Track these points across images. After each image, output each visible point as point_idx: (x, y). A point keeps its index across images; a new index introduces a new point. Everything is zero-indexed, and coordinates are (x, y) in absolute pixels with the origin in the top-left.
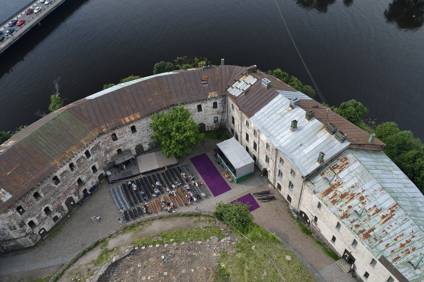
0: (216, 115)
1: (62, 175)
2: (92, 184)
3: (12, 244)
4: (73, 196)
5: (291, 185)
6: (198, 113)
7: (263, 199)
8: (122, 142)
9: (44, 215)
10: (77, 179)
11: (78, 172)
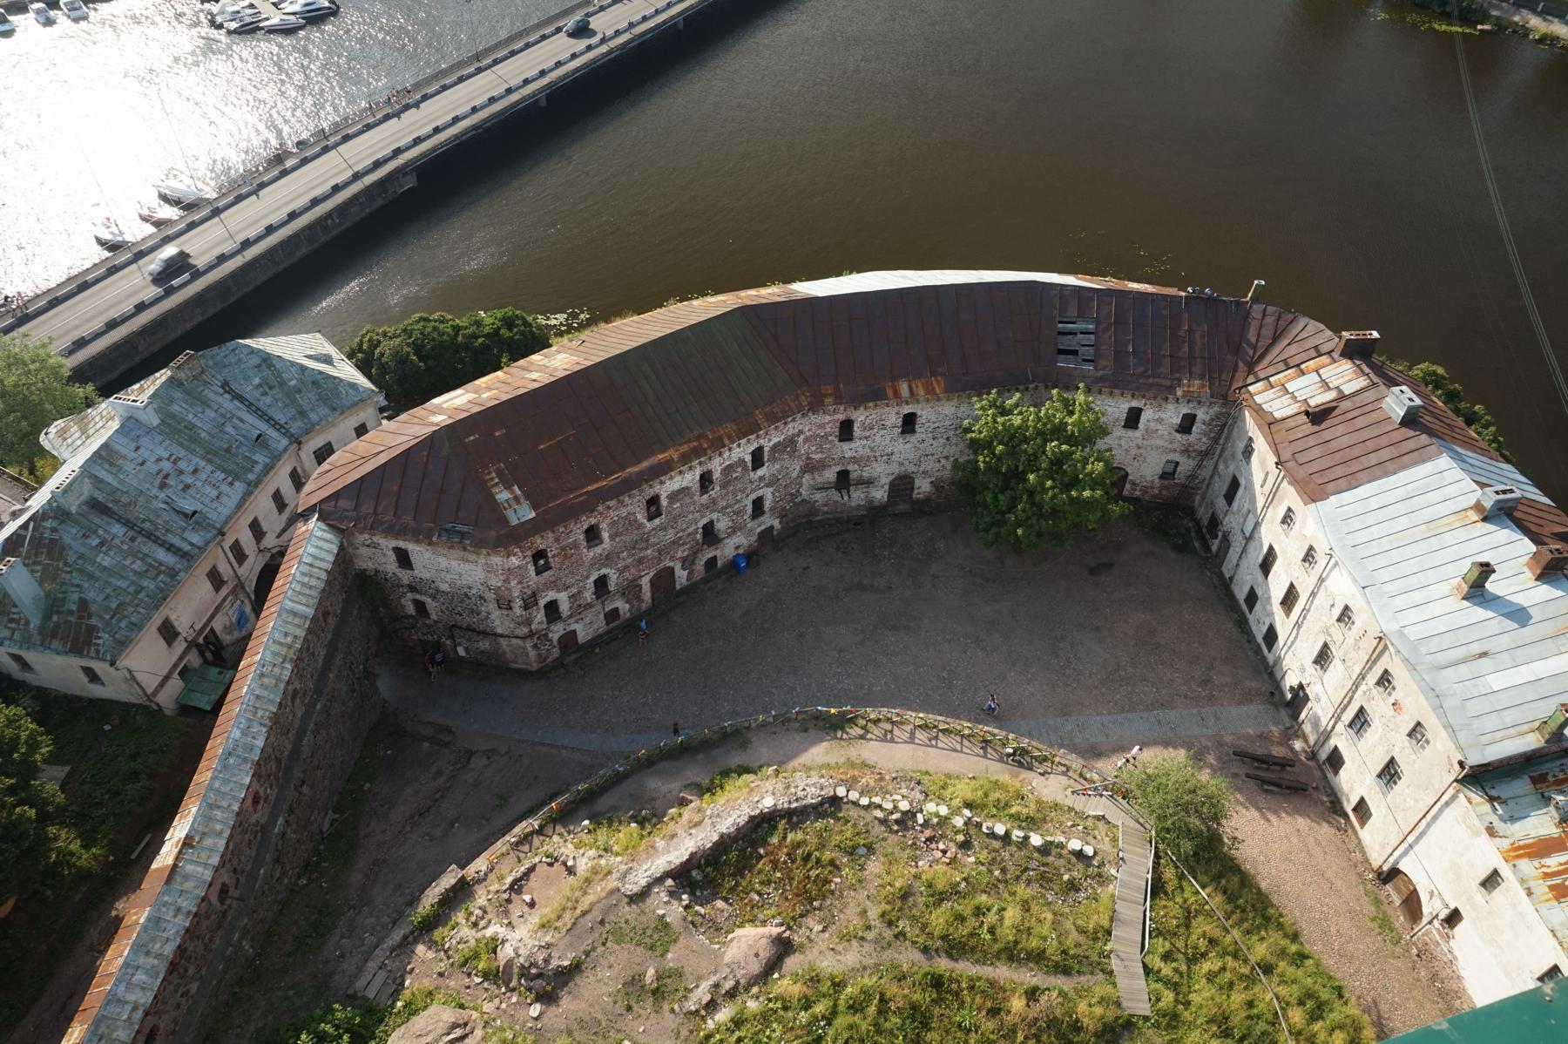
0: (1176, 457)
1: (673, 497)
2: (737, 548)
3: (485, 645)
4: (678, 567)
5: (1390, 773)
6: (1119, 431)
7: (1264, 782)
8: (861, 451)
9: (588, 595)
10: (705, 521)
11: (714, 501)
